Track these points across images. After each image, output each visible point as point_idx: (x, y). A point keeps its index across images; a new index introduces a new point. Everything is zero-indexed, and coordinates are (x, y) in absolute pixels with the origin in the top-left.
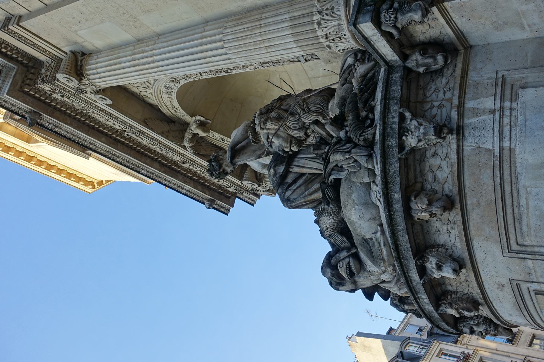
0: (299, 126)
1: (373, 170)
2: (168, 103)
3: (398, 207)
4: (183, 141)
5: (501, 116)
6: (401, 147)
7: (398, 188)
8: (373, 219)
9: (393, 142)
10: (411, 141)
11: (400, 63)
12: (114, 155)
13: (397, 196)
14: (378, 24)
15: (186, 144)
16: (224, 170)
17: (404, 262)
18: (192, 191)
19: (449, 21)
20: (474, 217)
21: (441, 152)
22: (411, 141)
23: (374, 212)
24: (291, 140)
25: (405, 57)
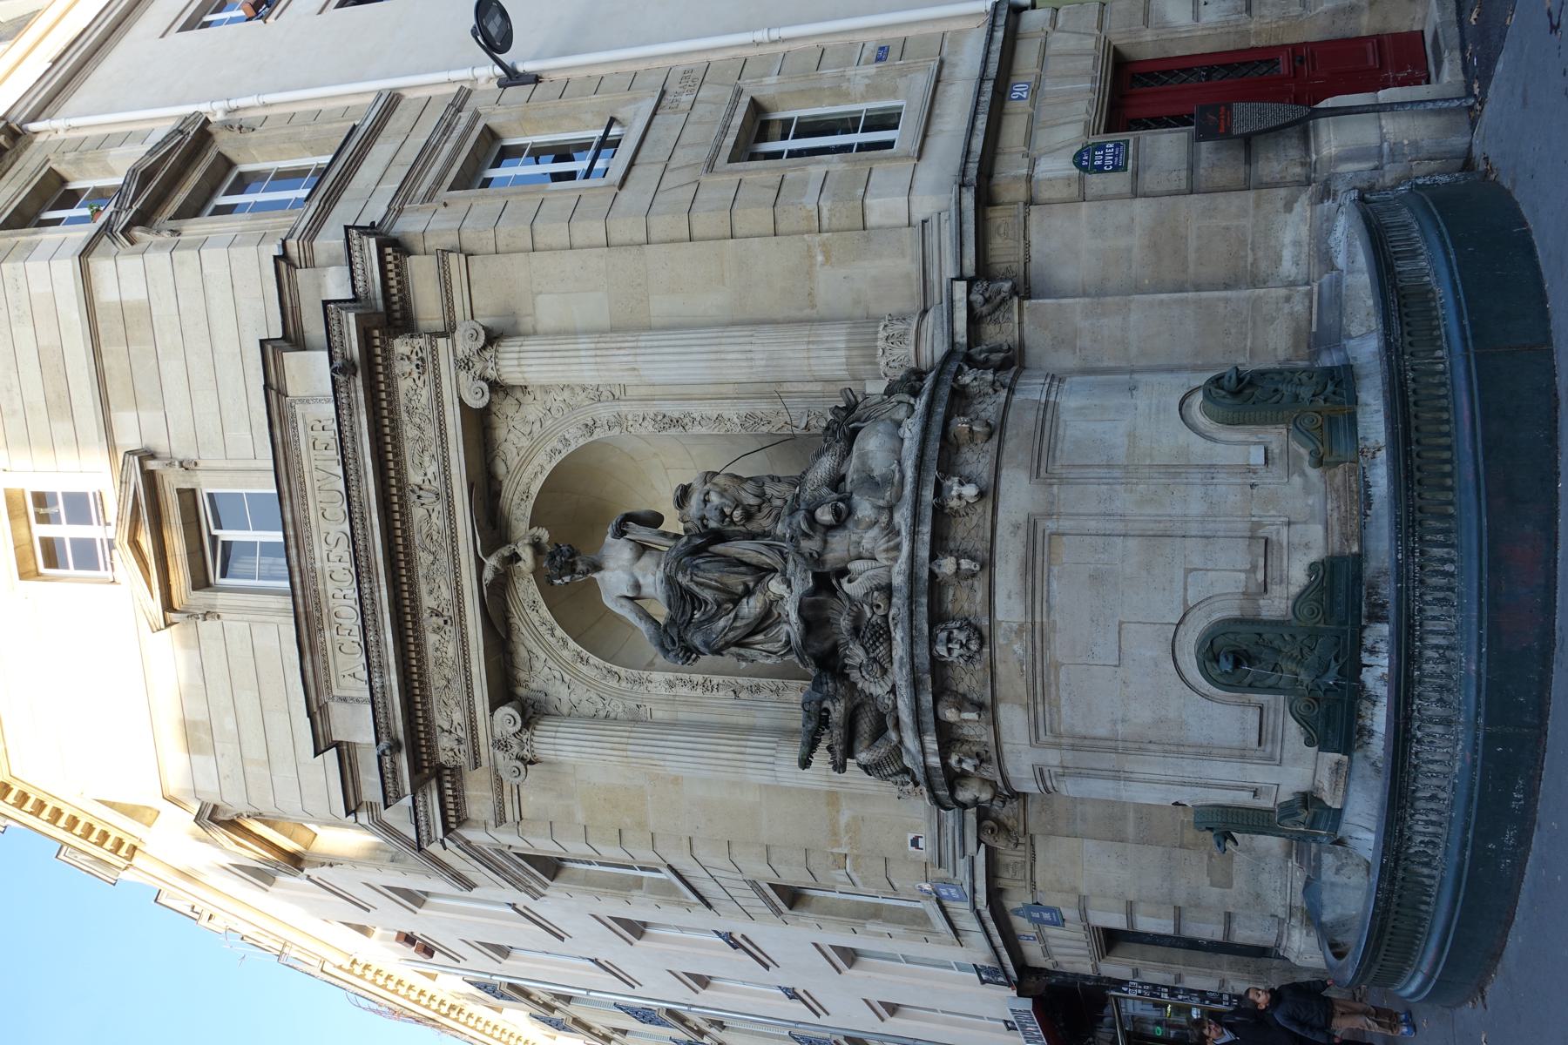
0: (758, 492)
1: (912, 408)
2: (525, 480)
3: (938, 418)
4: (487, 555)
5: (1050, 385)
6: (955, 379)
7: (943, 404)
8: (894, 451)
9: (949, 378)
10: (967, 379)
11: (964, 349)
12: (363, 519)
13: (940, 410)
14: (969, 292)
15: (492, 562)
16: (574, 563)
17: (924, 474)
18: (388, 696)
19: (1020, 323)
20: (1010, 445)
21: (988, 401)
22: (967, 379)
23: (897, 444)
24: (738, 504)
25: (969, 347)
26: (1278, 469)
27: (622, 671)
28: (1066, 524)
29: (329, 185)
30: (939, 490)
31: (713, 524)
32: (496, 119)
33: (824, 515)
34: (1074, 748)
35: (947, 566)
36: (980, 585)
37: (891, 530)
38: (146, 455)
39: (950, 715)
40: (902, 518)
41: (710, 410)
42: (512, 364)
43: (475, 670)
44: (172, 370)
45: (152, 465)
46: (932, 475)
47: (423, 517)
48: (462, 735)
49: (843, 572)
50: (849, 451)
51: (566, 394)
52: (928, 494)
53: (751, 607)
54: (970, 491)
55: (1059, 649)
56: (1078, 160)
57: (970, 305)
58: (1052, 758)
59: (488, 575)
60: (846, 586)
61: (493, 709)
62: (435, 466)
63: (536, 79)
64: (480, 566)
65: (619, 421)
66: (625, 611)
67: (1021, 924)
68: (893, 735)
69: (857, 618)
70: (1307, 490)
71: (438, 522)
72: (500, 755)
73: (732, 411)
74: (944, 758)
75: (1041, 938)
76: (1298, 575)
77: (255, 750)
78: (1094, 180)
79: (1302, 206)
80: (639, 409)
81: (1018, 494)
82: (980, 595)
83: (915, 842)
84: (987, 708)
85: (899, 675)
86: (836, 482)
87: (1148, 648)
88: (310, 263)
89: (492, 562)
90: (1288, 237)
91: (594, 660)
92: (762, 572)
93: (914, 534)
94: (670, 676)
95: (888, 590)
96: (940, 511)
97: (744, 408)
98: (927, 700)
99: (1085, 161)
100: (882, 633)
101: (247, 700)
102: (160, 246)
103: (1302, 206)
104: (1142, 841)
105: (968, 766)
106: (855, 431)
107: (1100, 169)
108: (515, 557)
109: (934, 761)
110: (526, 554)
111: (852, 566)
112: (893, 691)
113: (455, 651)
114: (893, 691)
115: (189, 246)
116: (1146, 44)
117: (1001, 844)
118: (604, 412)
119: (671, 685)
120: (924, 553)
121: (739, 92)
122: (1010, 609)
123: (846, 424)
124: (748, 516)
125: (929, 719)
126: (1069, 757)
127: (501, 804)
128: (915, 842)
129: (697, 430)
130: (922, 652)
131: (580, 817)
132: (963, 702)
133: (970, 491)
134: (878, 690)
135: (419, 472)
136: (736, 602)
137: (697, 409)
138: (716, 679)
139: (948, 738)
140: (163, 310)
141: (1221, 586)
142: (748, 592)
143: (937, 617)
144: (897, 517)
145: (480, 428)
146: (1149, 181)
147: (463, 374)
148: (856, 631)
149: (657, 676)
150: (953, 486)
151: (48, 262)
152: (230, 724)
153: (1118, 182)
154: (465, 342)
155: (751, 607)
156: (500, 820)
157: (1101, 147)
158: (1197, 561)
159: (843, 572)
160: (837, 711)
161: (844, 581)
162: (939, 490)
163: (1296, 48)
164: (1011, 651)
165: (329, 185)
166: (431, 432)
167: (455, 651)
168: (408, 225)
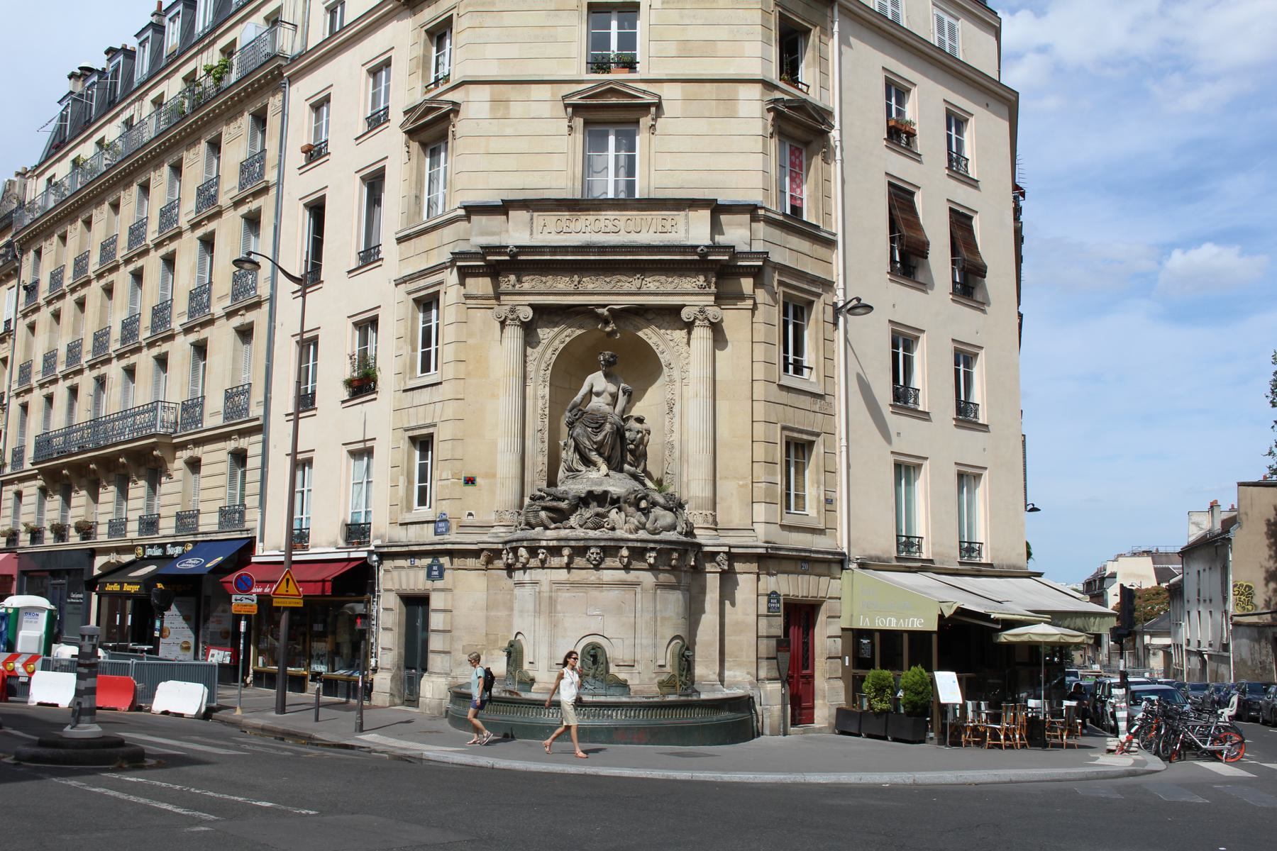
26: (658, 670)
27: (549, 372)
28: (639, 596)
29: (793, 223)
30: (653, 549)
31: (627, 434)
32: (818, 307)
33: (643, 504)
34: (550, 598)
35: (625, 552)
36: (620, 565)
37: (637, 530)
38: (659, 106)
39: (566, 552)
40: (642, 534)
41: (676, 427)
42: (701, 335)
43: (551, 298)
44: (701, 126)
45: (653, 109)
46: (658, 546)
48: (518, 286)
49: (620, 509)
50: (665, 508)
51: (685, 355)
52: (652, 545)
53: (594, 456)
54: (652, 561)
55: (595, 593)
56: (774, 593)
57: (718, 553)
58: (545, 587)
59: (600, 311)
60: (615, 510)
61: (530, 305)
63: (835, 324)
64: (604, 306)
65: (672, 381)
66: (585, 389)
67: (428, 561)
68: (553, 526)
69: (603, 516)
70: (651, 679)
71: (626, 287)
72: (508, 308)
73: (675, 437)
74: (543, 547)
75: (412, 566)
76: (622, 676)
77: (495, 145)
78: (763, 600)
79: (749, 678)
80: (677, 392)
81: (648, 578)
82: (614, 565)
83: (470, 514)
84: (568, 567)
85: (580, 533)
86: (655, 504)
87: (594, 625)
88: (753, 220)
89: (605, 311)
90: (738, 673)
91: (554, 357)
92: (608, 460)
93: (637, 541)
94: (547, 397)
95: (613, 529)
96: (645, 550)
97: (677, 444)
98: (573, 543)
99: (773, 596)
100: (598, 527)
101: (522, 145)
102: (765, 128)
103: (749, 678)
104: (487, 618)
105: (541, 556)
106: (671, 510)
107: (769, 602)
108: (607, 323)
109: (544, 543)
110: (608, 329)
111: (623, 514)
112: (572, 528)
114: (572, 528)
115: (765, 145)
116: (821, 618)
117: (483, 558)
118: (676, 374)
119: (543, 397)
120: (630, 544)
121: (818, 435)
122: (607, 575)
123: (676, 506)
124: (631, 451)
125: (562, 543)
126: (546, 595)
127: (476, 298)
128: (470, 514)
129: (667, 420)
130: (591, 543)
131: (470, 341)
132: (571, 557)
133: (652, 561)
134: (573, 521)
135: (652, 283)
136: (596, 450)
137: (677, 420)
138: (547, 420)
139: (555, 551)
140: (733, 126)
141: (616, 651)
142: (600, 455)
143: (603, 548)
144: (641, 532)
146: (763, 621)
147: (697, 309)
148: (597, 515)
149: (547, 389)
150: (653, 554)
151: (758, 56)
152: (509, 131)
153: (763, 609)
154: (713, 312)
155: (594, 456)
156: (467, 297)
157: (778, 602)
158: (627, 642)
159: (620, 509)
160: (564, 505)
161: (615, 510)
162: (653, 549)
163: (812, 676)
164: (592, 576)
165: (793, 223)
166: (669, 288)
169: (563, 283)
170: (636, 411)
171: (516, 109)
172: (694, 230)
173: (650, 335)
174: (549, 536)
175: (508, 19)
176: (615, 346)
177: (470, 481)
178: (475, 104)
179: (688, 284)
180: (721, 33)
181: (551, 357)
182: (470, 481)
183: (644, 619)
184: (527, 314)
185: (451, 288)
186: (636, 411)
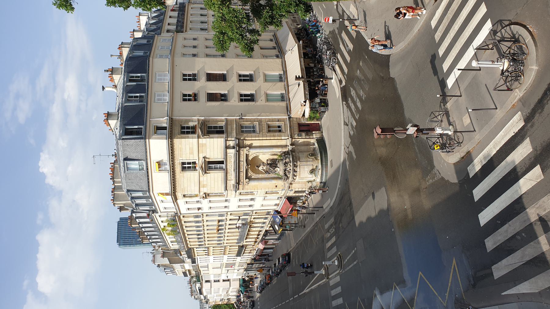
38: (204, 158)
47: (242, 163)
62: (243, 158)
113: (243, 175)
122: (298, 170)
145: (247, 156)
167: (243, 175)
168: (238, 137)
169: (241, 174)
170: (265, 162)
171: (205, 183)
172: (232, 152)
173: (250, 158)
174: (291, 179)
175: (186, 186)
176: (253, 164)
177: (276, 186)
178: (204, 190)
179: (242, 152)
180: (188, 147)
181: (254, 175)
182: (276, 186)
183: (305, 163)
184: (247, 180)
185: (241, 190)
186: (265, 162)
